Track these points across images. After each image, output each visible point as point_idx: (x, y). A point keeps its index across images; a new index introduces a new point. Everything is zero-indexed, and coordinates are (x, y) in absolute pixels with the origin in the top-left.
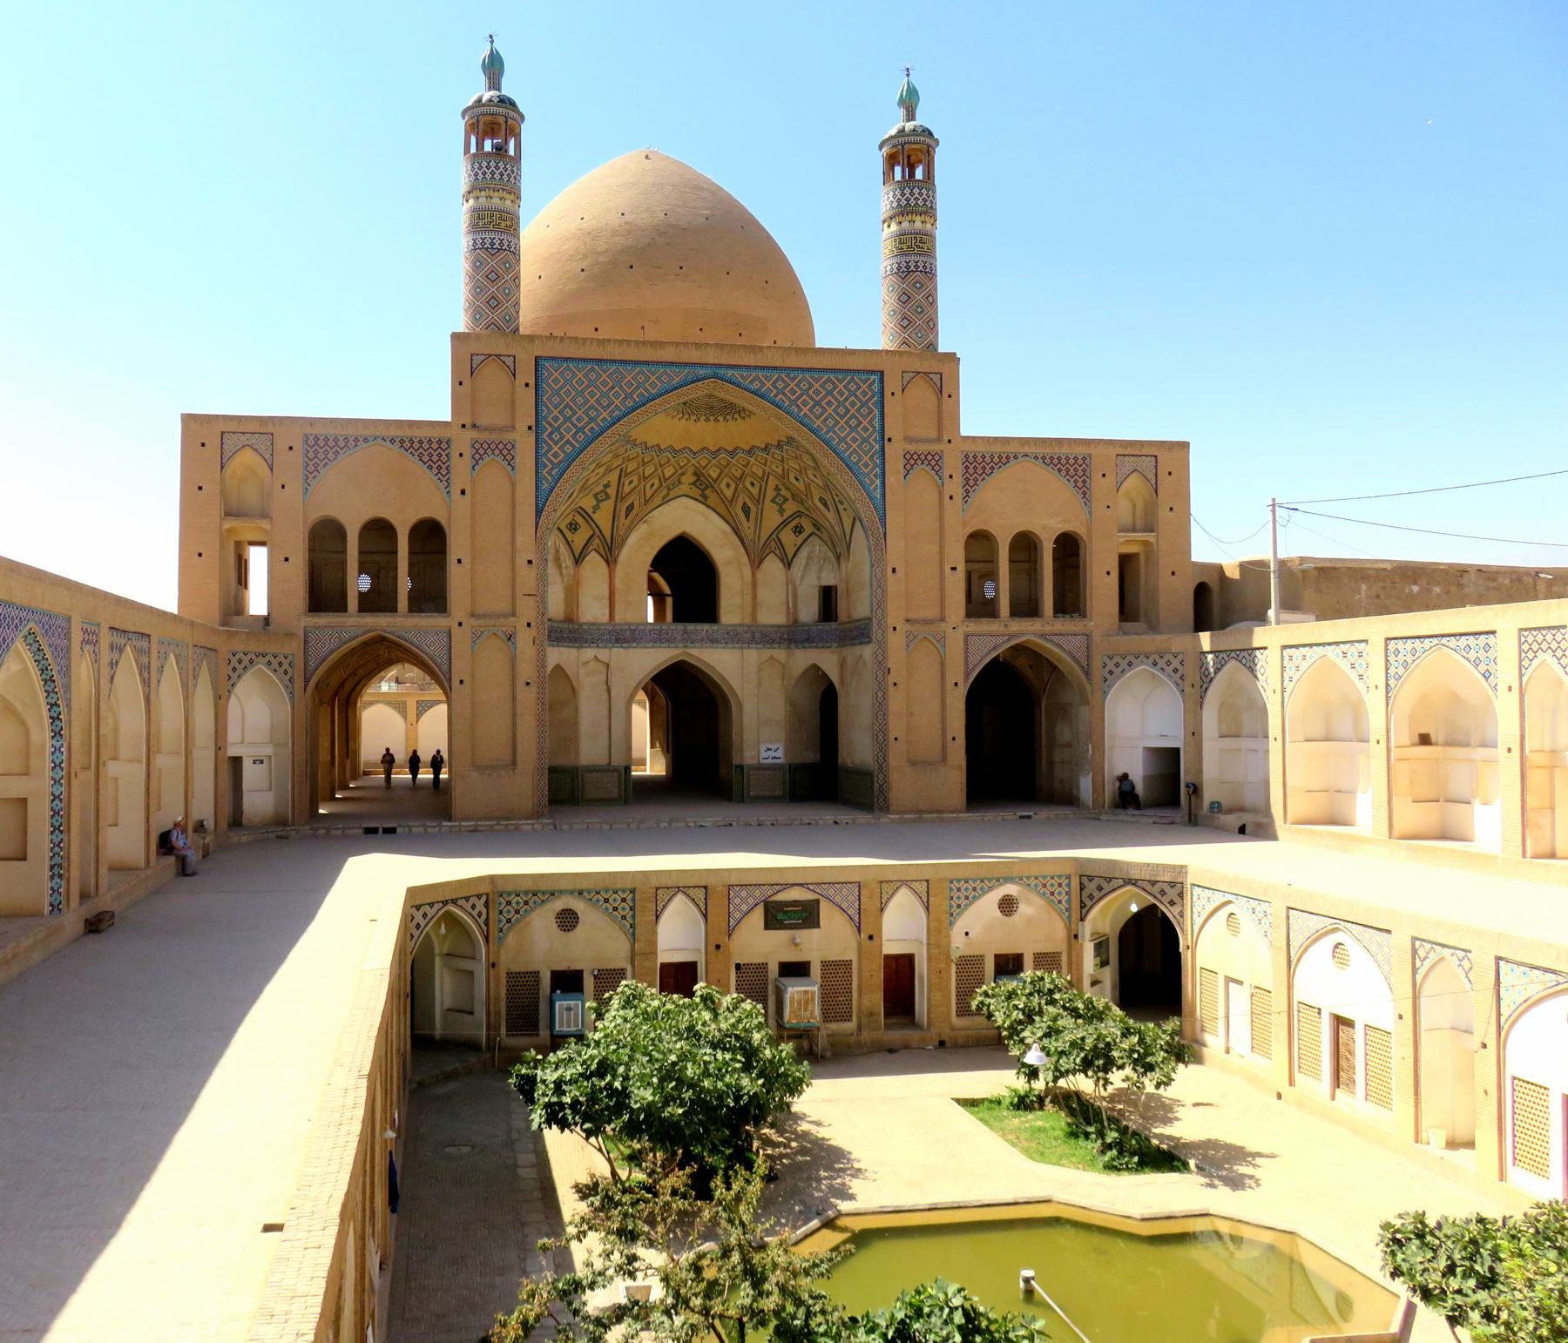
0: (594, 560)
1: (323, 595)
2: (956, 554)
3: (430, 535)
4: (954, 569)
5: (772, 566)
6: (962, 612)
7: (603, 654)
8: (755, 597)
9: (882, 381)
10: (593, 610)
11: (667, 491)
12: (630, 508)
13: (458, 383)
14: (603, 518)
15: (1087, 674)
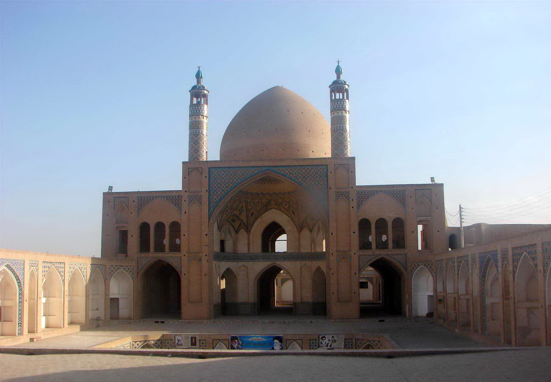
0: (243, 232)
1: (144, 246)
2: (355, 227)
3: (175, 227)
4: (354, 232)
5: (306, 232)
6: (357, 247)
7: (245, 264)
8: (299, 243)
9: (327, 168)
10: (242, 248)
11: (266, 208)
12: (252, 214)
13: (184, 178)
14: (243, 217)
15: (406, 269)
